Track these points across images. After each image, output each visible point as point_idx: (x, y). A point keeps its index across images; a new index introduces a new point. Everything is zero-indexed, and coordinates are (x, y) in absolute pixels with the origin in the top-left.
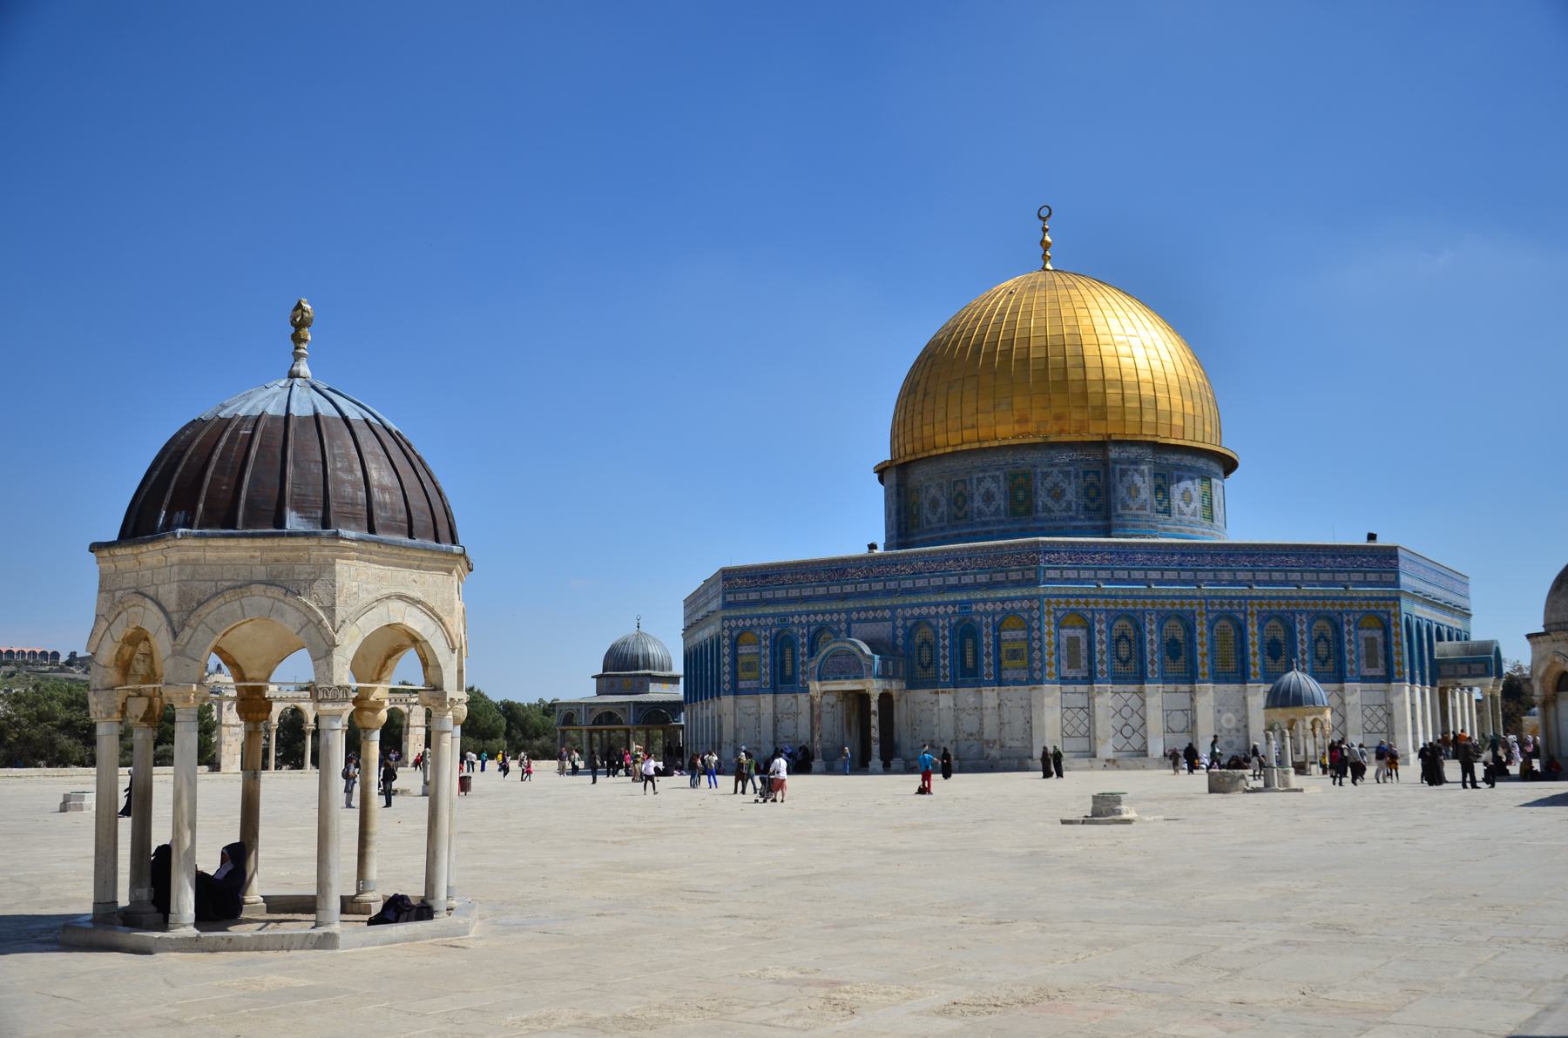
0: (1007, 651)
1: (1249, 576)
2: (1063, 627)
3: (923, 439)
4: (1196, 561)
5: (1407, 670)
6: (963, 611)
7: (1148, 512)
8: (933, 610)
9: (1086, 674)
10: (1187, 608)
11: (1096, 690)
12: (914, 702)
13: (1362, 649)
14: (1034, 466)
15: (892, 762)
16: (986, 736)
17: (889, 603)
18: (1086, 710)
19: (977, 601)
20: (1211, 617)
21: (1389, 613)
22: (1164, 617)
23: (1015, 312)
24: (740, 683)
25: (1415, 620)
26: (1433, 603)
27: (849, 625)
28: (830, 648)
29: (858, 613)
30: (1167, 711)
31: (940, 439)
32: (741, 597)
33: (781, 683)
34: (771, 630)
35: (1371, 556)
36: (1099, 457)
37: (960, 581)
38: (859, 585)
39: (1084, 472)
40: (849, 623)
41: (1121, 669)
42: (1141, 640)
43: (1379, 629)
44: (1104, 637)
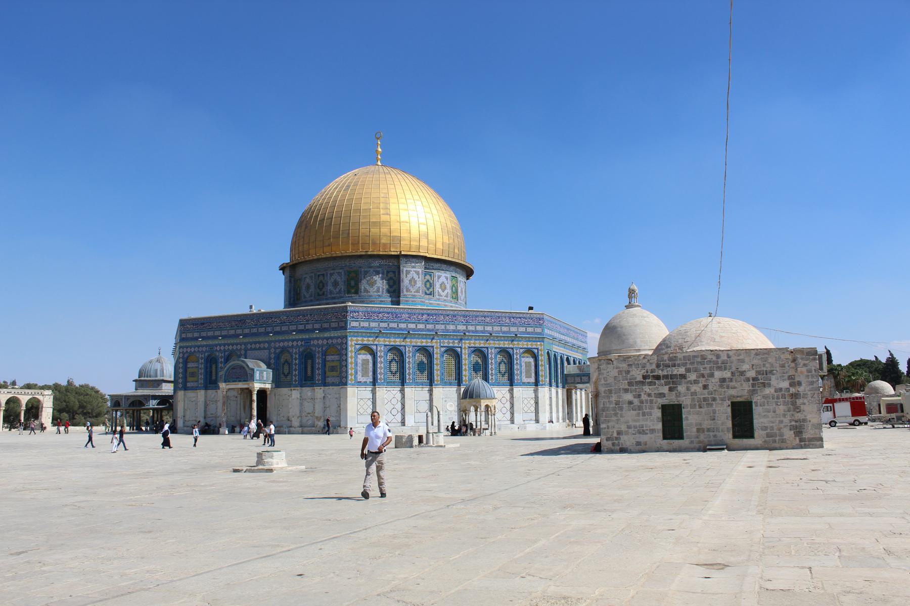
0: (329, 367)
1: (464, 328)
5: (548, 379)
7: (420, 294)
8: (290, 344)
12: (279, 395)
13: (524, 367)
14: (360, 267)
16: (316, 414)
19: (314, 339)
21: (538, 349)
23: (355, 185)
24: (188, 383)
25: (553, 353)
26: (565, 344)
29: (251, 345)
32: (190, 335)
33: (210, 384)
36: (396, 264)
37: (305, 327)
38: (252, 329)
39: (387, 271)
40: (246, 350)
44: (382, 360)
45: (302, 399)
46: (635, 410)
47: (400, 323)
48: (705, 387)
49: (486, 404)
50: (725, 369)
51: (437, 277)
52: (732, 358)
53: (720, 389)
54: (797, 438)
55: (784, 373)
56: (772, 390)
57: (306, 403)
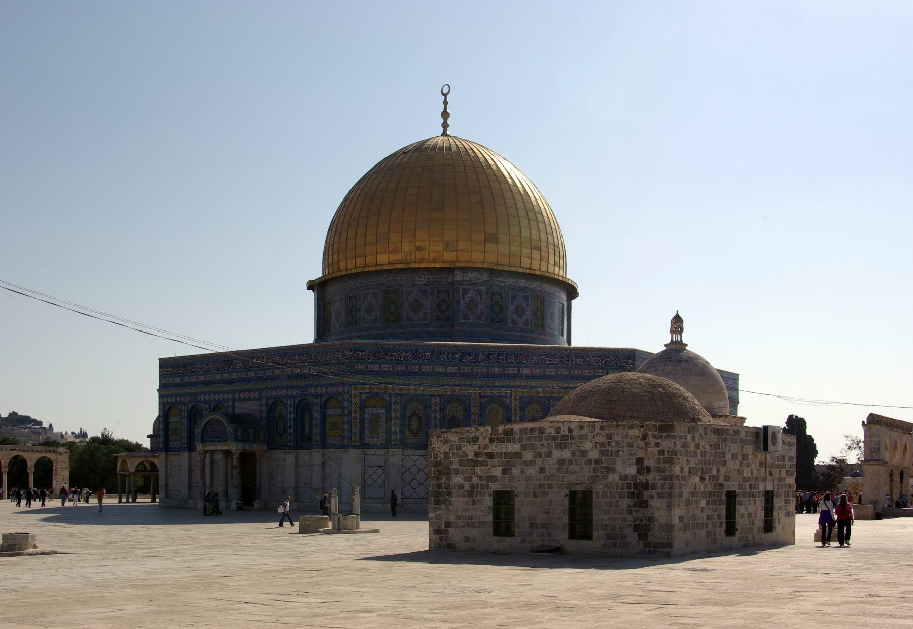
1: (515, 370)
3: (333, 264)
6: (302, 393)
9: (384, 442)
11: (390, 453)
15: (254, 502)
17: (257, 387)
18: (383, 468)
24: (170, 443)
27: (234, 402)
31: (342, 265)
32: (170, 381)
34: (188, 405)
35: (613, 357)
39: (438, 290)
44: (398, 415)
45: (297, 464)
46: (465, 496)
47: (423, 364)
48: (542, 470)
50: (565, 447)
51: (510, 298)
52: (574, 433)
53: (558, 474)
54: (641, 542)
55: (631, 455)
56: (617, 478)
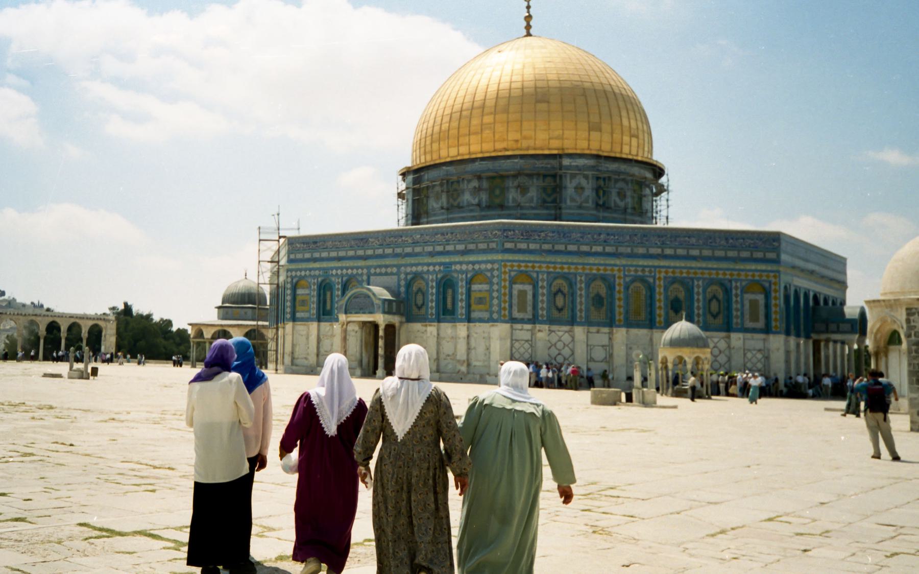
0: (475, 298)
1: (659, 251)
2: (515, 283)
4: (618, 239)
8: (425, 268)
9: (531, 317)
10: (609, 272)
18: (530, 342)
19: (456, 263)
20: (628, 279)
22: (591, 279)
28: (349, 295)
30: (590, 346)
32: (299, 256)
33: (324, 315)
41: (555, 314)
42: (573, 294)
43: (761, 293)
44: (545, 291)
49: (696, 355)
57: (444, 343)
